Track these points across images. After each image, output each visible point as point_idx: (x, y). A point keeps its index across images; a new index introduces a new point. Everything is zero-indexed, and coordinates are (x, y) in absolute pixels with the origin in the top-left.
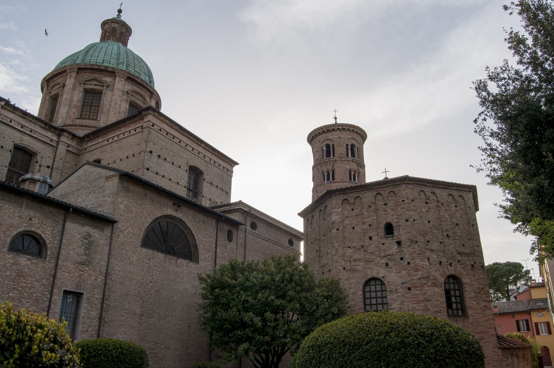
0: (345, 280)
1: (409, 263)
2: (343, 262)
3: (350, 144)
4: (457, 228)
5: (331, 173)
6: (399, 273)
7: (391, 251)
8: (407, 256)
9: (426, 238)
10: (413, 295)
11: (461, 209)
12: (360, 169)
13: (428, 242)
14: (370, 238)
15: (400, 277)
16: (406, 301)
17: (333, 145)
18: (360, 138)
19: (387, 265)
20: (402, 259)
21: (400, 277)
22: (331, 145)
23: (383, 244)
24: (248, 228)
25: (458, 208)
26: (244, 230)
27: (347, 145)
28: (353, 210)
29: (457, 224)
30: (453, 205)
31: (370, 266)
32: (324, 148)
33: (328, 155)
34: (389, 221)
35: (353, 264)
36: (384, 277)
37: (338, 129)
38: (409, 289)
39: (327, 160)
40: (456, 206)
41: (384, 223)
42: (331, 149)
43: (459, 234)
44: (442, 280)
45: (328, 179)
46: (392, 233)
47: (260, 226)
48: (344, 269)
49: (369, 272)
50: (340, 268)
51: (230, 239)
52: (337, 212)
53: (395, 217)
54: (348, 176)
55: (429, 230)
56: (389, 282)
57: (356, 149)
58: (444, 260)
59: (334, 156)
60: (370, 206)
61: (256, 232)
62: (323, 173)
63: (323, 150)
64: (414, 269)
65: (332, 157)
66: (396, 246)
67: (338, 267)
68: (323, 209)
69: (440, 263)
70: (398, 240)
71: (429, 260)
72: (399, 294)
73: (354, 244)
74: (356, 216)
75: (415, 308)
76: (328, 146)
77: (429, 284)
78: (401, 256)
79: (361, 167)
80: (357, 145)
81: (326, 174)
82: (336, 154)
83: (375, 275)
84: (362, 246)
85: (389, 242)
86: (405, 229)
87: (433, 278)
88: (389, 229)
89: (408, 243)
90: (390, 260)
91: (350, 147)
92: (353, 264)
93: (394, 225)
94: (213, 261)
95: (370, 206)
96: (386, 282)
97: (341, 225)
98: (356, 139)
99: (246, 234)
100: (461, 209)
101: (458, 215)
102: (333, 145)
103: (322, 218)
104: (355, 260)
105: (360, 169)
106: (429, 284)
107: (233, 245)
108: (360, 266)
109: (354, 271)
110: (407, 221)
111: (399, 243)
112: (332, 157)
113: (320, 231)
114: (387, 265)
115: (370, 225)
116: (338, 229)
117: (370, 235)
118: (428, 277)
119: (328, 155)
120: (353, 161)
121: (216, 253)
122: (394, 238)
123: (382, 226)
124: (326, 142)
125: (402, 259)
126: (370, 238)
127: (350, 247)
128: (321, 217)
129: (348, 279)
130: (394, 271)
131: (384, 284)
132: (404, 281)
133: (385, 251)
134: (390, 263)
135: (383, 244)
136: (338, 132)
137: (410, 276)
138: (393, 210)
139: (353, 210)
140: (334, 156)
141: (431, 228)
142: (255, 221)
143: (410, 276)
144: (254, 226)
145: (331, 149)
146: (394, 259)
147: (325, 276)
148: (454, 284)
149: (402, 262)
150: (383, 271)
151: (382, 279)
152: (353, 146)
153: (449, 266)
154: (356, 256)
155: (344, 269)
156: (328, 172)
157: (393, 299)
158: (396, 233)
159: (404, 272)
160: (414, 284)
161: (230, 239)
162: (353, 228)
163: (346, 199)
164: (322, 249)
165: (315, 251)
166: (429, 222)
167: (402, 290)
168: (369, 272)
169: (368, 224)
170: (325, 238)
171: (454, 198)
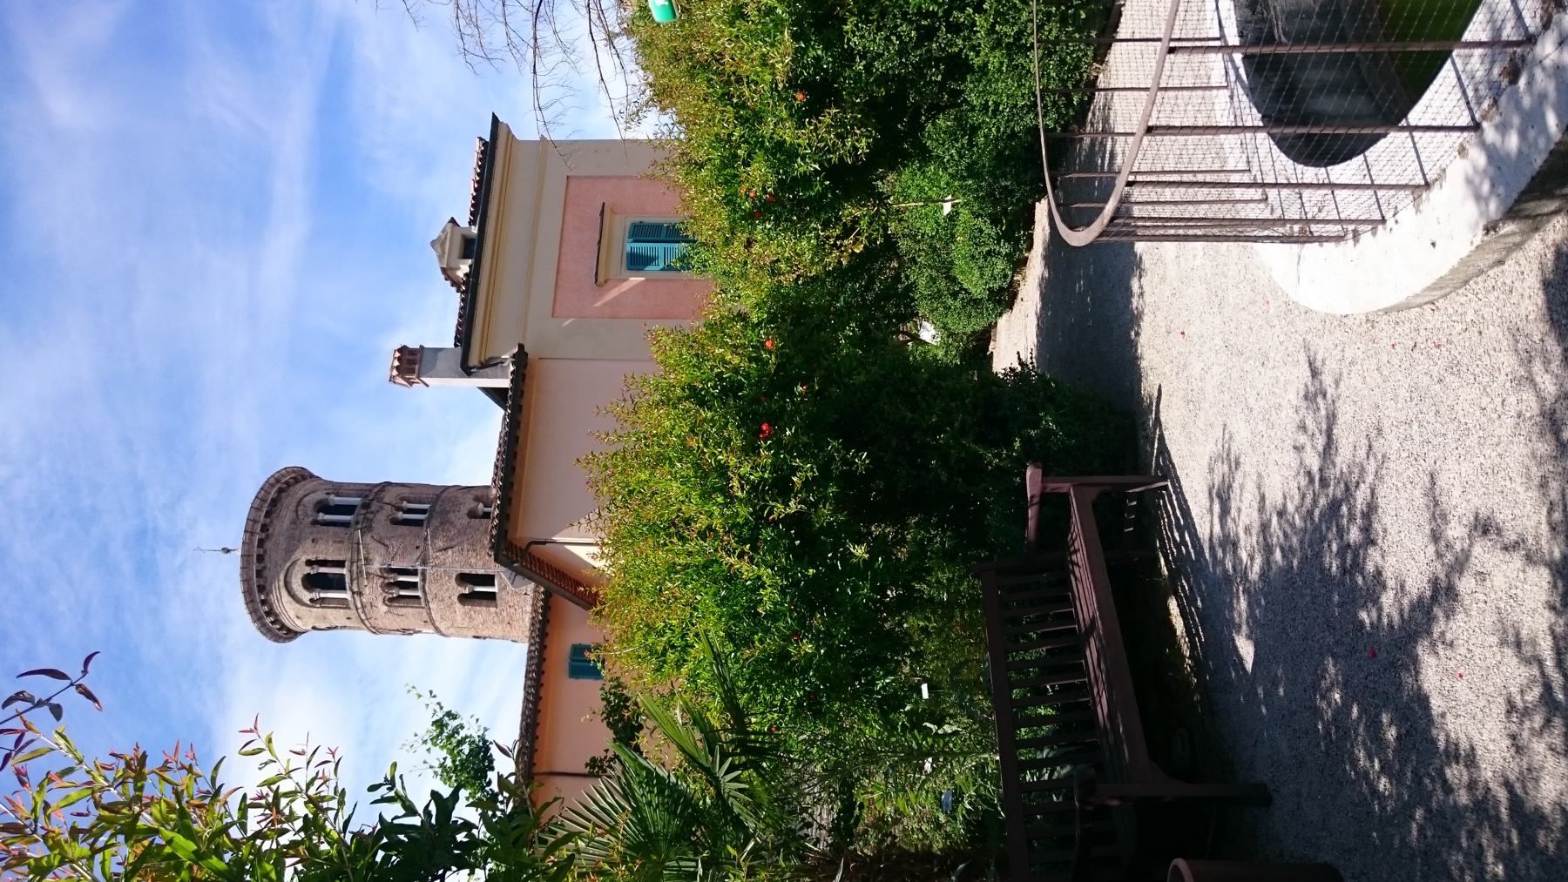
5: (392, 578)
17: (309, 563)
22: (308, 570)
27: (315, 522)
32: (315, 595)
33: (337, 583)
37: (261, 543)
42: (323, 570)
45: (413, 586)
62: (391, 600)
65: (344, 571)
76: (311, 582)
81: (395, 592)
91: (322, 516)
102: (309, 563)
112: (344, 571)
124: (297, 585)
136: (268, 545)
140: (341, 564)
145: (323, 570)
152: (323, 507)
156: (390, 585)
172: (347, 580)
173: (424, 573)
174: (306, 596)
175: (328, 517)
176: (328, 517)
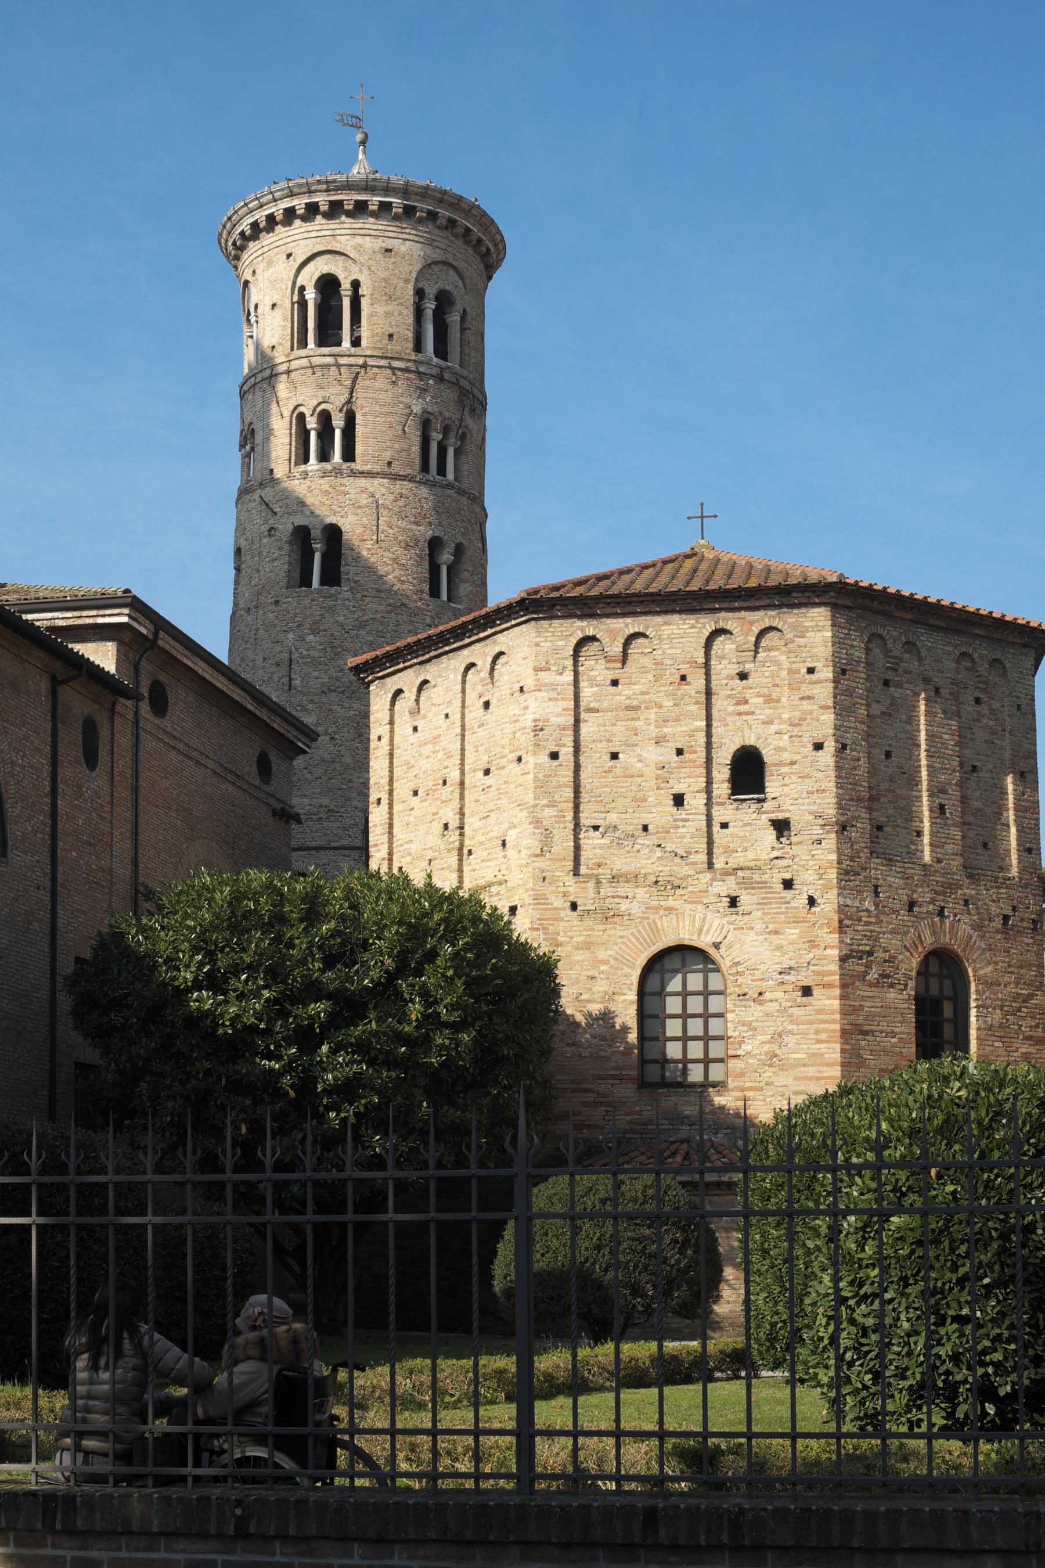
0: (577, 948)
1: (812, 901)
2: (570, 880)
3: (431, 291)
4: (972, 784)
6: (777, 932)
7: (750, 855)
8: (809, 876)
9: (875, 814)
10: (819, 1012)
11: (993, 712)
12: (469, 421)
13: (880, 828)
14: (679, 800)
15: (779, 948)
16: (791, 1032)
17: (356, 285)
18: (478, 265)
19: (733, 902)
20: (788, 884)
21: (779, 948)
22: (346, 286)
23: (724, 826)
24: (145, 707)
25: (984, 709)
26: (130, 716)
28: (615, 683)
29: (974, 768)
30: (968, 697)
31: (670, 903)
32: (311, 295)
34: (751, 740)
35: (607, 890)
36: (717, 946)
38: (807, 991)
39: (322, 355)
40: (978, 701)
41: (734, 748)
42: (346, 303)
43: (977, 804)
44: (913, 963)
46: (760, 788)
47: (179, 697)
48: (574, 906)
49: (664, 922)
50: (558, 902)
51: (91, 759)
52: (553, 687)
53: (774, 728)
54: (416, 449)
55: (884, 786)
56: (737, 964)
57: (454, 318)
58: (923, 895)
59: (356, 342)
60: (683, 678)
61: (166, 723)
62: (301, 417)
63: (303, 304)
64: (828, 925)
65: (346, 343)
66: (771, 834)
67: (552, 899)
68: (484, 663)
69: (912, 904)
70: (781, 816)
71: (877, 894)
72: (770, 1007)
73: (613, 818)
74: (629, 708)
75: (822, 1055)
77: (873, 975)
78: (788, 876)
79: (473, 411)
80: (462, 300)
82: (365, 331)
83: (686, 936)
84: (645, 828)
85: (747, 819)
86: (808, 777)
87: (887, 956)
88: (748, 772)
89: (817, 831)
90: (747, 884)
91: (430, 306)
92: (607, 890)
93: (768, 755)
94: (47, 849)
95: (683, 678)
96: (725, 964)
97: (569, 741)
98: (461, 265)
99: (137, 736)
100: (993, 712)
101: (981, 735)
102: (356, 285)
103: (474, 702)
104: (614, 878)
105: (469, 421)
106: (873, 975)
107: (97, 782)
108: (637, 900)
109: (608, 916)
110: (818, 747)
111: (781, 827)
112: (346, 343)
113: (463, 749)
114: (733, 902)
115: (680, 752)
116: (554, 756)
117: (678, 789)
118: (870, 953)
119: (328, 334)
120: (440, 379)
121: (54, 815)
122: (767, 806)
123: (723, 757)
125: (788, 884)
126: (679, 800)
127: (596, 828)
128: (471, 697)
129: (588, 945)
130: (759, 926)
131: (718, 970)
132: (792, 964)
133: (728, 851)
134: (746, 899)
135: (724, 826)
137: (812, 944)
138: (769, 700)
139: (615, 683)
140: (356, 342)
141: (891, 779)
142: (163, 678)
143: (812, 944)
144: (160, 704)
145: (346, 303)
146: (763, 885)
147: (911, 984)
148: (941, 977)
149: (788, 894)
150: (716, 923)
151: (712, 951)
153: (937, 919)
154: (620, 863)
155: (574, 906)
157: (749, 1025)
158: (772, 787)
159: (793, 933)
160: (824, 974)
161: (91, 759)
162: (614, 756)
163: (593, 639)
164: (472, 823)
165: (438, 827)
166: (888, 755)
167: (779, 995)
168: (664, 922)
169: (672, 747)
170: (489, 780)
171: (973, 669)
172: (335, 350)
173: (337, 472)
174: (309, 277)
175: (429, 314)
176: (429, 314)
